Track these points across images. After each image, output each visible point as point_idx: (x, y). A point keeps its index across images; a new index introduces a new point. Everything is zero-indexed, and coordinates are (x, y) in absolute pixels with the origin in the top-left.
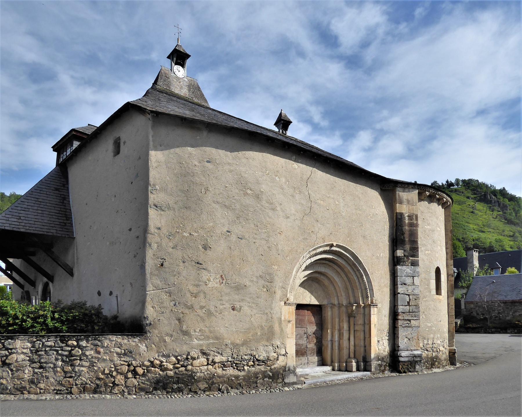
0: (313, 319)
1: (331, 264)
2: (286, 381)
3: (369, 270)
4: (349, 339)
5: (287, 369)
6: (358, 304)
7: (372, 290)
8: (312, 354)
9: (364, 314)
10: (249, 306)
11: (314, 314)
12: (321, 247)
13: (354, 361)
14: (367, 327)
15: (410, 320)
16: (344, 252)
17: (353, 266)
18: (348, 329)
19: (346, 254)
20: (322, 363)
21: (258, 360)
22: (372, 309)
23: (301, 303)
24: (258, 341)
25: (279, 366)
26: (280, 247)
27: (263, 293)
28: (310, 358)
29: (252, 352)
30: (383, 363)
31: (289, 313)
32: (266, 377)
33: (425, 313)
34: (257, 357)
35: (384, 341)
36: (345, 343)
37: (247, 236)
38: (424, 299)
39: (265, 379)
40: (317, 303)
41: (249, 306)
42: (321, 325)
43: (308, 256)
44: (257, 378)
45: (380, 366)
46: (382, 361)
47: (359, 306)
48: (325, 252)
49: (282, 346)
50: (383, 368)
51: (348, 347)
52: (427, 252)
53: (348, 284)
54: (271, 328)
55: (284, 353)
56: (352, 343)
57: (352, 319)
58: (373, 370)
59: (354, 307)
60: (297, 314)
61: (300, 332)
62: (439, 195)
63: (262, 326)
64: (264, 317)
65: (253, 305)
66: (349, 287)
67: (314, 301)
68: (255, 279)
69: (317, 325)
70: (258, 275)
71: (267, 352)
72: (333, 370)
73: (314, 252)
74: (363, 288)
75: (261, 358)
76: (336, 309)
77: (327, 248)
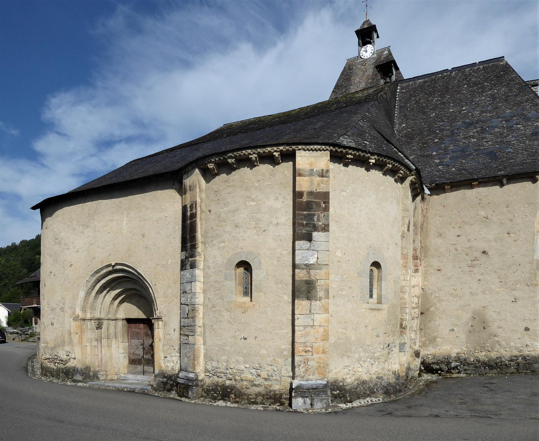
15: (188, 336)
25: (69, 366)
30: (169, 381)
33: (214, 326)
38: (213, 309)
45: (165, 384)
46: (168, 379)
49: (72, 351)
50: (168, 386)
52: (222, 244)
62: (231, 157)
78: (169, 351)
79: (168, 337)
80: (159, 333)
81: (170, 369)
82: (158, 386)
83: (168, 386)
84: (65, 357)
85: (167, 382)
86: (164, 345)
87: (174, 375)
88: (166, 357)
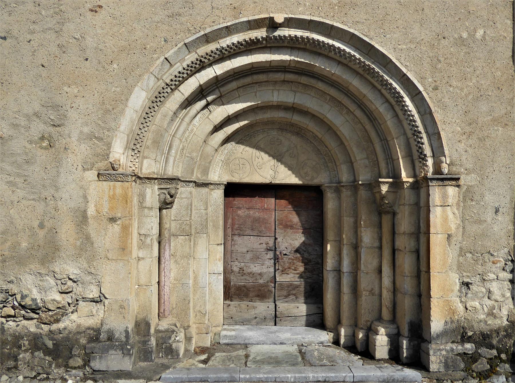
0: (295, 219)
1: (304, 80)
2: (96, 364)
3: (422, 79)
4: (380, 271)
5: (103, 336)
6: (396, 175)
7: (435, 136)
8: (292, 297)
9: (417, 204)
10: (9, 183)
11: (297, 208)
12: (229, 30)
13: (382, 330)
14: (423, 239)
16: (321, 38)
17: (365, 74)
18: (377, 244)
19: (331, 42)
20: (317, 321)
21: (24, 307)
22: (436, 193)
23: (236, 179)
24: (21, 261)
25: (72, 326)
26: (90, 42)
27: (40, 152)
28: (282, 306)
29: (10, 286)
30: (483, 351)
31: (112, 198)
32: (38, 349)
34: (18, 297)
35: (494, 287)
36: (366, 282)
37: (15, 33)
39: (36, 354)
40: (293, 180)
41: (9, 183)
42: (316, 232)
43: (191, 58)
44: (20, 347)
45: (471, 359)
47: (397, 184)
48: (251, 47)
49: (89, 278)
50: (482, 365)
51: (377, 291)
53: (368, 127)
54: (54, 231)
55: (94, 294)
56: (387, 281)
57: (386, 220)
58: (435, 364)
59: (384, 189)
60: (227, 206)
61: (256, 246)
63: (31, 229)
64: (40, 207)
65: (17, 180)
66: (373, 135)
67: (286, 176)
68: (23, 122)
69: (306, 231)
70: (31, 112)
71: (42, 289)
72: (336, 342)
73: (213, 47)
74: (409, 134)
75: (28, 302)
76: (346, 193)
77: (261, 33)
78: (480, 269)
79: (473, 229)
80: (445, 219)
81: (483, 317)
82: (447, 366)
83: (482, 365)
84: (58, 297)
85: (476, 352)
86: (462, 252)
87: (497, 332)
88: (467, 285)
